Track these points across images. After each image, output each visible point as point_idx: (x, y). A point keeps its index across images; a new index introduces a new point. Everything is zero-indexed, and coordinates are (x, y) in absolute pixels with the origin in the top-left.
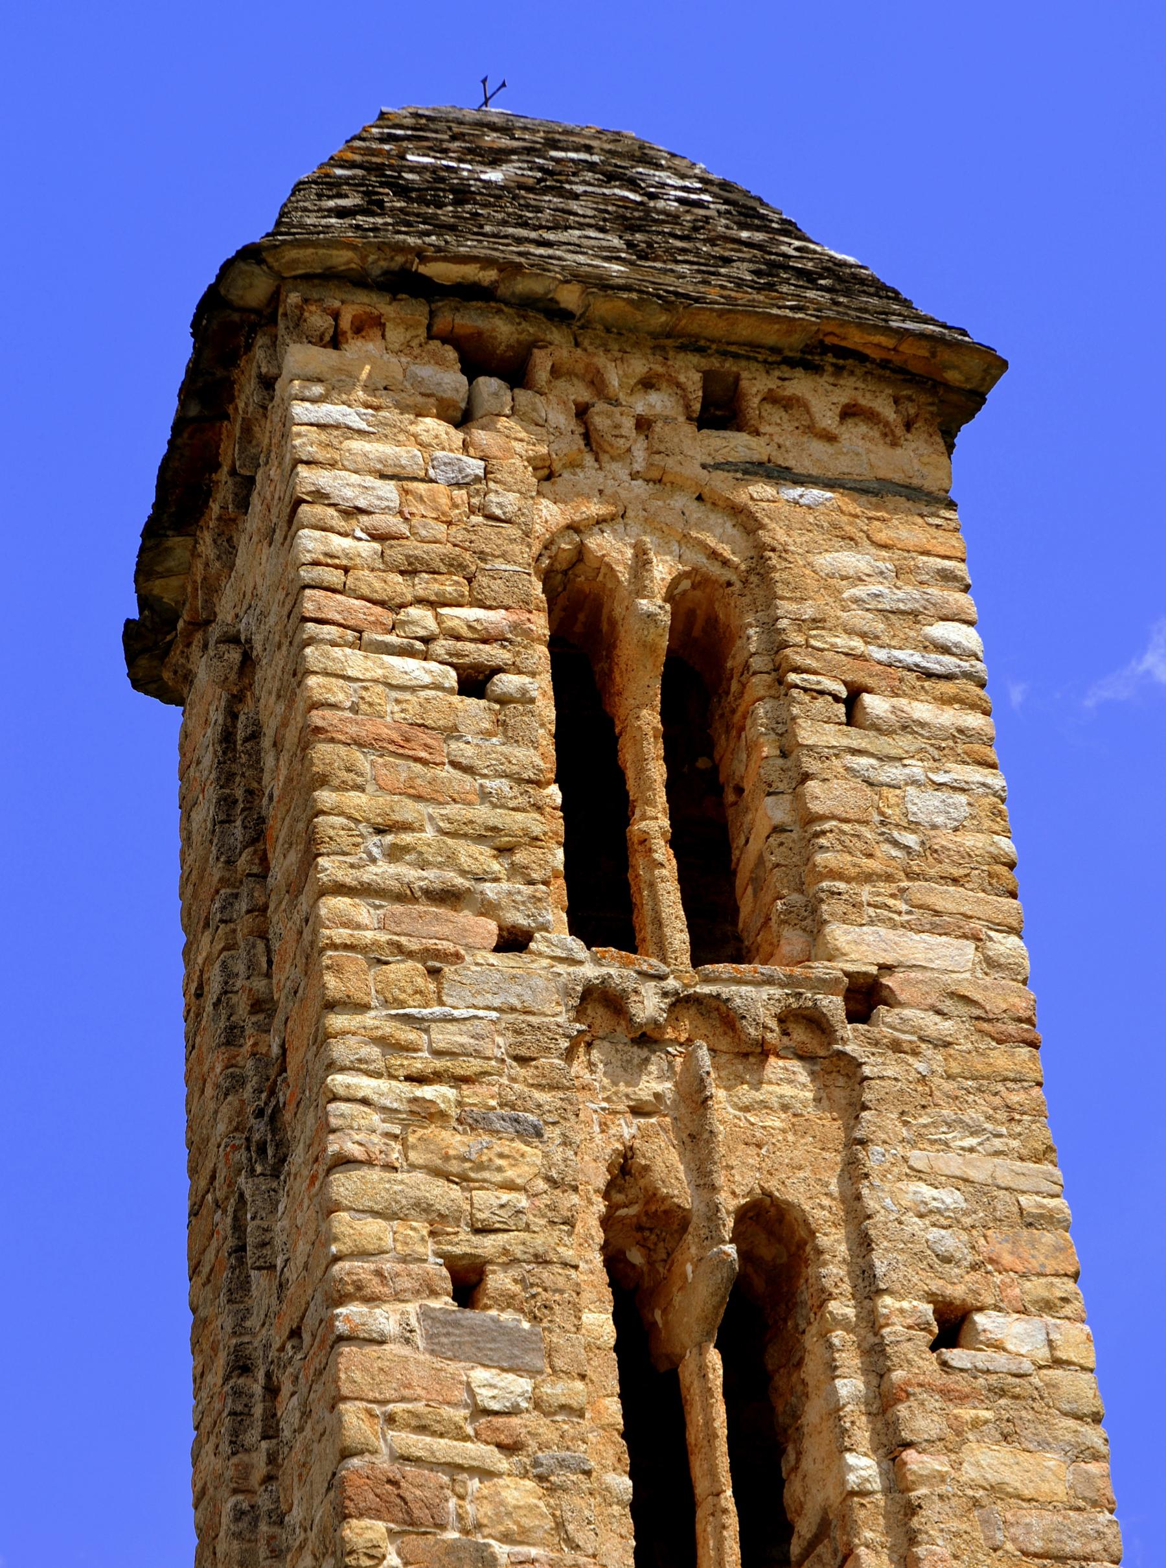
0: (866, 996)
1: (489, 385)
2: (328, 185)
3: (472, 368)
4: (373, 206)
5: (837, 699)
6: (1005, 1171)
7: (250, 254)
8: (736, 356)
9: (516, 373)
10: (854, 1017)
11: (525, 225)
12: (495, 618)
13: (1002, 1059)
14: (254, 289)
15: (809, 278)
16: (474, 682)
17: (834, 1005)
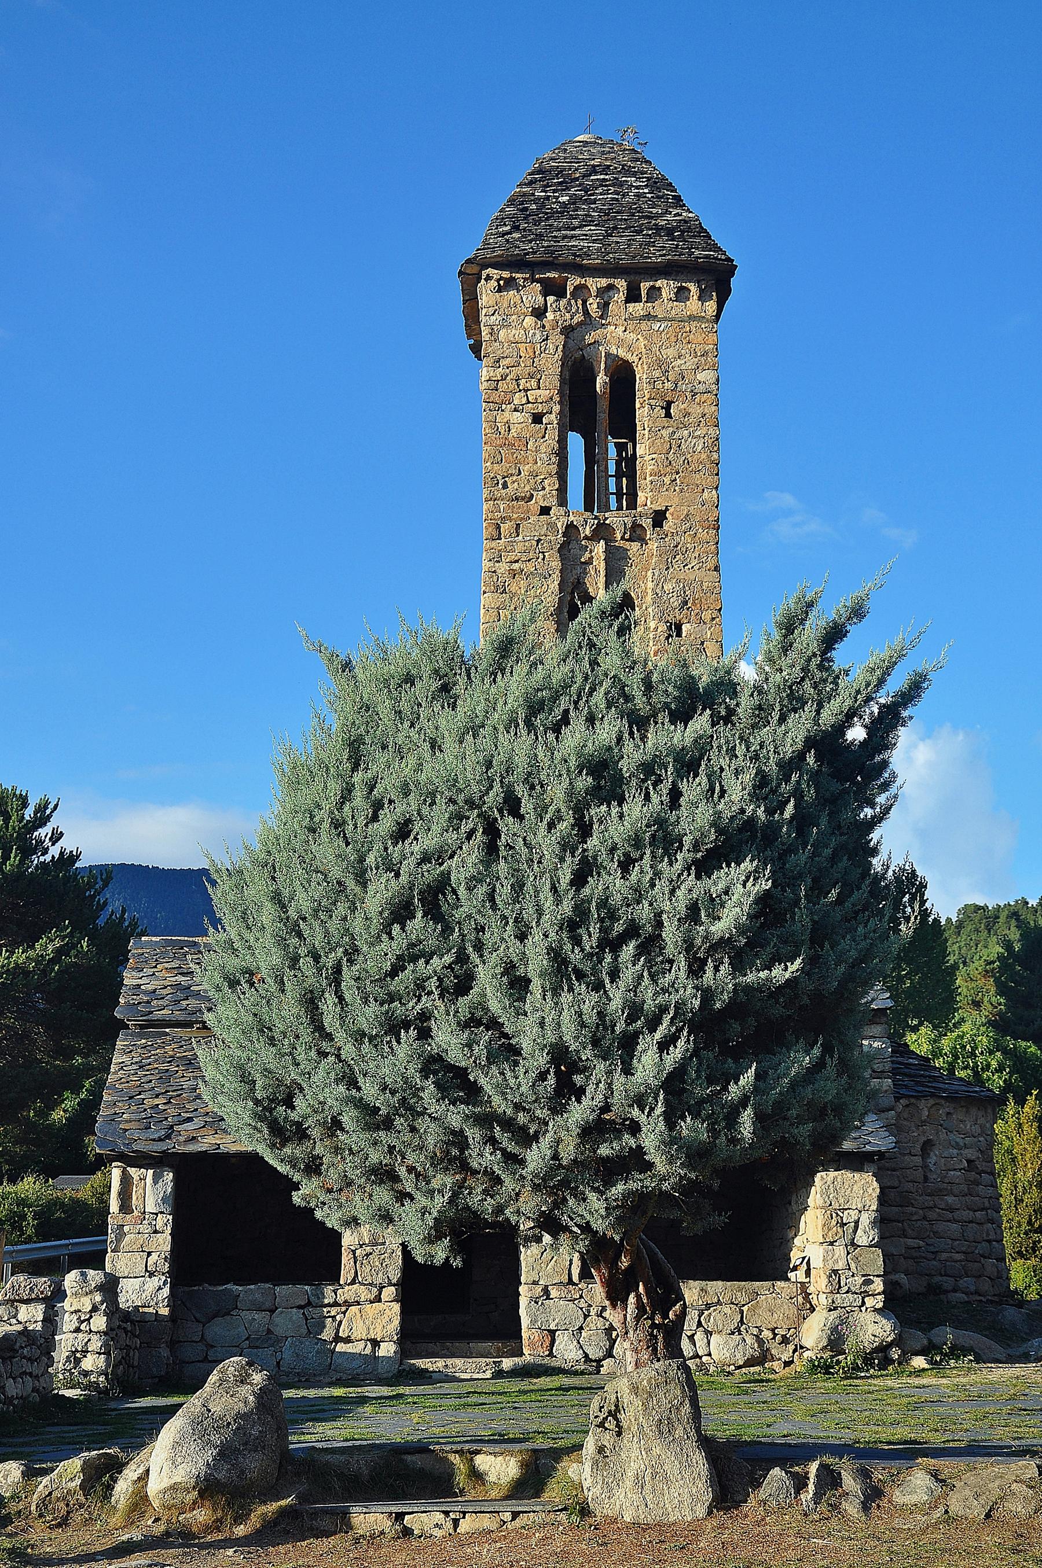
0: (659, 518)
1: (551, 299)
2: (501, 220)
3: (545, 295)
4: (516, 228)
5: (662, 408)
6: (700, 574)
7: (469, 261)
8: (640, 273)
9: (560, 294)
10: (654, 526)
11: (569, 228)
12: (544, 394)
13: (702, 534)
14: (473, 269)
15: (670, 232)
16: (537, 419)
17: (647, 523)
